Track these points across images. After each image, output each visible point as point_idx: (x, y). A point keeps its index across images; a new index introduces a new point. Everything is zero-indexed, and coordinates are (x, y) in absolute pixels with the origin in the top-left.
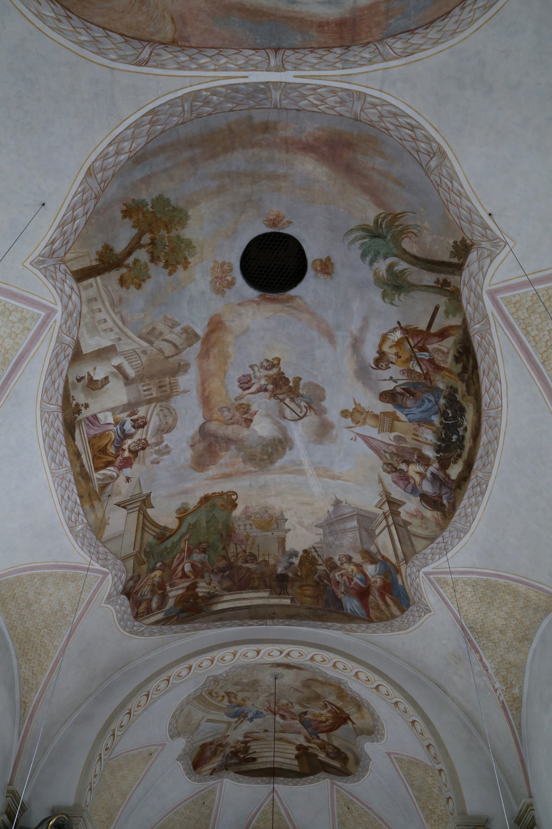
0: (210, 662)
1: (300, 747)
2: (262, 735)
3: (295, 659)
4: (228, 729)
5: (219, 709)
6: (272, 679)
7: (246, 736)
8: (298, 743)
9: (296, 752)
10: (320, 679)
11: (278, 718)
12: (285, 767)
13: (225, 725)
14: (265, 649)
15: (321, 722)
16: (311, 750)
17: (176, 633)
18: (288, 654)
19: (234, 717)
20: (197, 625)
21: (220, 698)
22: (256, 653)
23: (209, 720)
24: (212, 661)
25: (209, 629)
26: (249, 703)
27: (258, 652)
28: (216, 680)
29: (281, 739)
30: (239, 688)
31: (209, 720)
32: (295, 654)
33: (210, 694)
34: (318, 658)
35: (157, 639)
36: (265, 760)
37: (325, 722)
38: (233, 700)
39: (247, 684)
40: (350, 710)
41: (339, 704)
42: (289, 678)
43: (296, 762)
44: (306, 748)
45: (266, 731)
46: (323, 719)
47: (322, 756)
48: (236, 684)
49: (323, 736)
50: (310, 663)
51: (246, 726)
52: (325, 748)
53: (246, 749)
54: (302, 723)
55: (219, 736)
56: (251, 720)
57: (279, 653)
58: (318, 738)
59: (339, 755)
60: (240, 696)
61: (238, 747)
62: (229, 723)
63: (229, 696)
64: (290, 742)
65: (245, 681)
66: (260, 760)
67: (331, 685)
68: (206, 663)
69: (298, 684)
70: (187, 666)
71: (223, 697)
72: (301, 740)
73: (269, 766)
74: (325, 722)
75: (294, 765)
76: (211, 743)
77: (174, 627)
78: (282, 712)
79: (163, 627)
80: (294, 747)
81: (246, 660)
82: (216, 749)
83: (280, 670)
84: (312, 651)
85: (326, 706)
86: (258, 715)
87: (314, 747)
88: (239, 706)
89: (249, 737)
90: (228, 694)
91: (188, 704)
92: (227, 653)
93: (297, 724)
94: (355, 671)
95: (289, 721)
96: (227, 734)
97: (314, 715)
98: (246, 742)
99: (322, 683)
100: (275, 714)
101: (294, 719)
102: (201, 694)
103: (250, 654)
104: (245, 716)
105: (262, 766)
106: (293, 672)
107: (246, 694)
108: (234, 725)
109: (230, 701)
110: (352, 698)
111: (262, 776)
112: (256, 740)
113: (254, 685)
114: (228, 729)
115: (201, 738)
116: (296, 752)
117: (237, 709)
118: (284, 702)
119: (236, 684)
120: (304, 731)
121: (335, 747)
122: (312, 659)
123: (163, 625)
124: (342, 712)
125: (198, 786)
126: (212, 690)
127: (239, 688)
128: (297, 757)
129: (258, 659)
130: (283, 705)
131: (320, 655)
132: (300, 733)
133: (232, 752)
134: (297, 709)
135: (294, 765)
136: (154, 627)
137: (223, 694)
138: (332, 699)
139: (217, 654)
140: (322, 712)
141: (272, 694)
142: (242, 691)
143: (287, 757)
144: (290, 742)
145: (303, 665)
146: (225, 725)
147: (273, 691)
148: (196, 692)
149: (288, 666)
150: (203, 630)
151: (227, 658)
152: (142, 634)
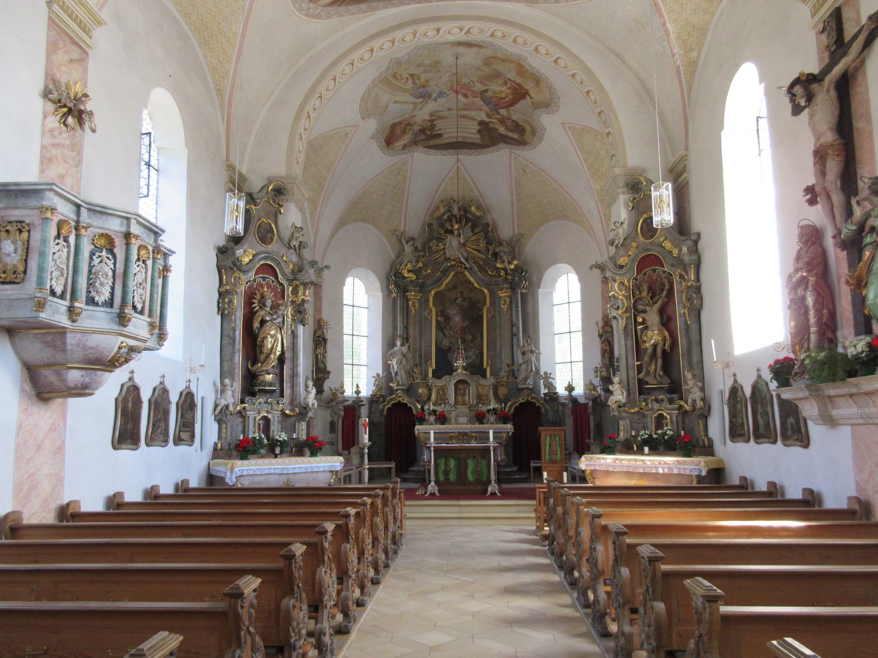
0: (391, 44)
1: (481, 123)
2: (446, 113)
3: (475, 37)
4: (414, 109)
5: (405, 91)
6: (453, 59)
7: (431, 115)
8: (480, 119)
9: (478, 128)
10: (500, 55)
11: (460, 97)
12: (468, 140)
13: (412, 106)
14: (446, 26)
15: (501, 98)
16: (491, 125)
17: (353, 14)
18: (468, 31)
19: (419, 97)
20: (374, 4)
21: (405, 80)
22: (436, 32)
23: (396, 102)
24: (393, 42)
25: (387, 8)
26: (432, 84)
27: (438, 30)
28: (398, 62)
29: (464, 117)
30: (422, 69)
31: (396, 102)
32: (475, 31)
33: (394, 76)
34: (499, 34)
35: (335, 21)
36: (450, 135)
37: (504, 98)
38: (417, 81)
39: (430, 66)
40: (529, 86)
41: (519, 80)
42: (469, 57)
43: (478, 136)
44: (488, 123)
45: (449, 109)
46: (503, 95)
47: (502, 130)
48: (419, 66)
49: (503, 112)
50: (489, 39)
51: (431, 106)
52: (504, 122)
53: (433, 127)
54: (483, 100)
55: (406, 116)
56: (435, 100)
57: (458, 30)
58: (498, 113)
59: (518, 128)
60: (423, 78)
61: (425, 125)
62: (415, 104)
63: (412, 76)
64: (472, 119)
65: (427, 62)
66: (445, 136)
67: (511, 62)
68: (387, 45)
69: (479, 62)
70: (368, 48)
71: (407, 79)
72: (483, 117)
73: (454, 140)
74: (504, 98)
75: (476, 138)
76: (400, 123)
77: (351, 8)
78: (464, 91)
79: (340, 8)
80: (476, 123)
81: (427, 40)
82: (405, 129)
83: (461, 49)
84: (493, 27)
85: (506, 83)
86: (441, 94)
87: (494, 122)
88: (424, 87)
89: (434, 117)
90: (412, 76)
91: (374, 87)
92: (406, 33)
93: (478, 101)
94: (535, 45)
95: (471, 99)
96: (414, 113)
97: (494, 92)
98: (432, 121)
99: (503, 61)
100: (457, 92)
101: (475, 97)
102: (386, 78)
103: (430, 33)
104: (430, 96)
105: (447, 141)
106: (474, 50)
107: (429, 75)
108: (419, 106)
109: (414, 83)
110: (531, 73)
111: (448, 149)
112: (441, 118)
113: (436, 66)
114: (414, 109)
115: (390, 119)
116: (478, 128)
117: (421, 90)
118: (465, 81)
119: (419, 66)
120: (485, 108)
121: (514, 121)
122: (492, 35)
123: (339, 5)
124: (522, 88)
125: (394, 159)
126: (396, 73)
127: (422, 69)
128: (479, 132)
129: (439, 38)
130: (465, 84)
131: (500, 30)
132: (481, 110)
133: (420, 130)
134: (479, 87)
135: (476, 138)
136: (330, 9)
137: (407, 76)
138: (512, 75)
139: (398, 35)
140: (502, 89)
141: (453, 74)
142: (425, 72)
143: (470, 131)
144: (472, 119)
145: (484, 42)
146: (412, 106)
147: (454, 71)
148: (381, 75)
149: (469, 45)
150: (380, 9)
151: (408, 39)
152: (319, 16)
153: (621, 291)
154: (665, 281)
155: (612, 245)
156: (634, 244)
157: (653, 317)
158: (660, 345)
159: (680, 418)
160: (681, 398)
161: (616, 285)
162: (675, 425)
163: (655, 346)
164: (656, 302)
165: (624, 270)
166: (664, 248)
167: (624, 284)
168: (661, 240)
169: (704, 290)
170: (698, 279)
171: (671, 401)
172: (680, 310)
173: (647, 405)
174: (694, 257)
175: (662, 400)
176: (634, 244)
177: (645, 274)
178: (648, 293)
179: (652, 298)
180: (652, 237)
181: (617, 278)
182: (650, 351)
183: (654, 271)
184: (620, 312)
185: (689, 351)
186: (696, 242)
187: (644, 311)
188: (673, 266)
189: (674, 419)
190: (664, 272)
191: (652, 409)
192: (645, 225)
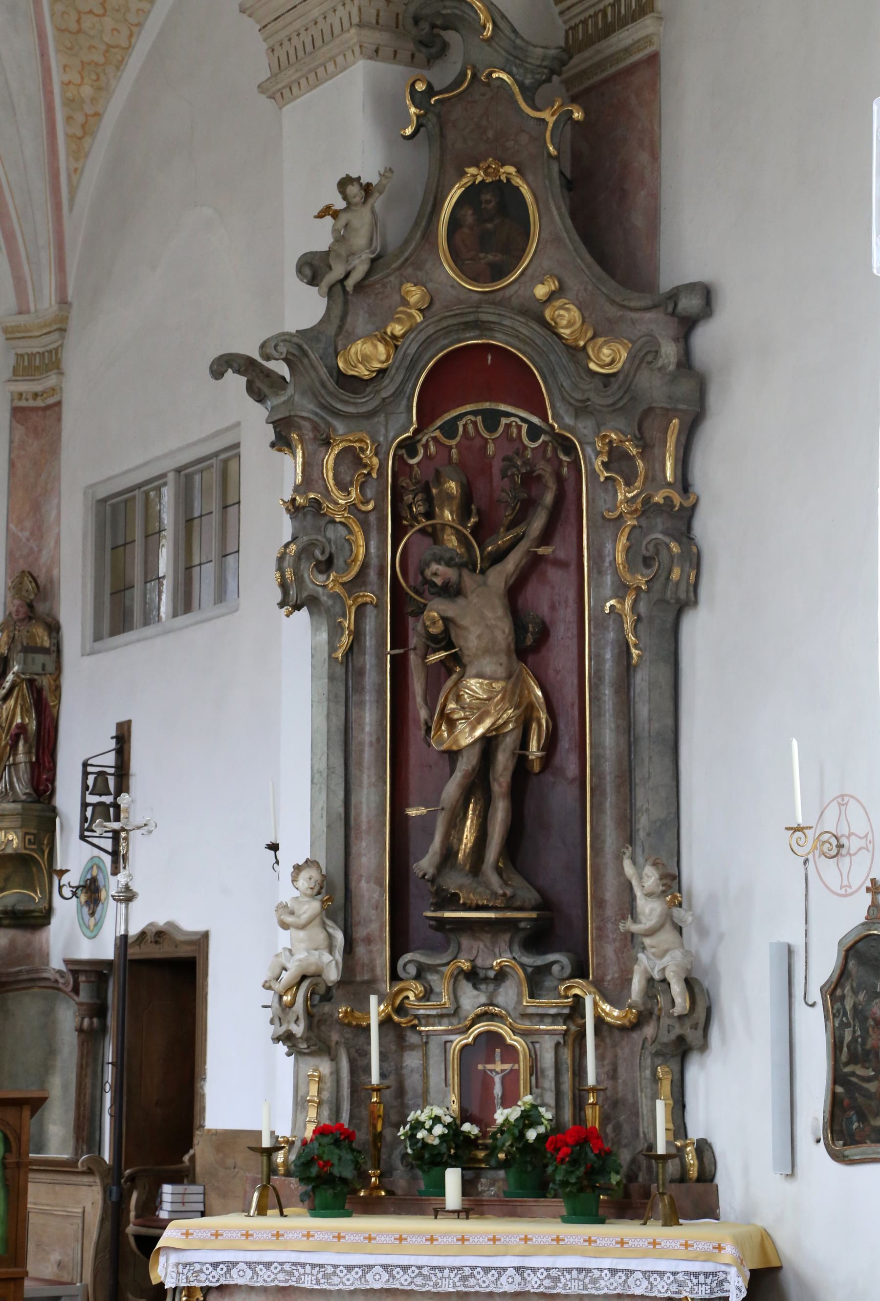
153: (343, 487)
154: (545, 469)
155: (313, 281)
156: (415, 294)
157: (481, 621)
158: (508, 744)
159: (567, 1055)
160: (580, 971)
161: (330, 460)
162: (549, 1083)
163: (488, 744)
164: (499, 557)
165: (366, 403)
166: (551, 329)
167: (359, 463)
168: (541, 291)
169: (709, 527)
170: (684, 484)
171: (536, 981)
172: (605, 599)
173: (428, 994)
174: (685, 387)
175: (501, 975)
176: (415, 294)
177: (449, 429)
178: (464, 513)
179: (481, 532)
180: (498, 272)
181: (340, 427)
182: (466, 765)
183: (492, 419)
184: (332, 581)
185: (627, 779)
186: (687, 325)
187: (451, 591)
188: (582, 410)
189: (548, 1059)
190: (534, 432)
191: (456, 1012)
192: (469, 216)
